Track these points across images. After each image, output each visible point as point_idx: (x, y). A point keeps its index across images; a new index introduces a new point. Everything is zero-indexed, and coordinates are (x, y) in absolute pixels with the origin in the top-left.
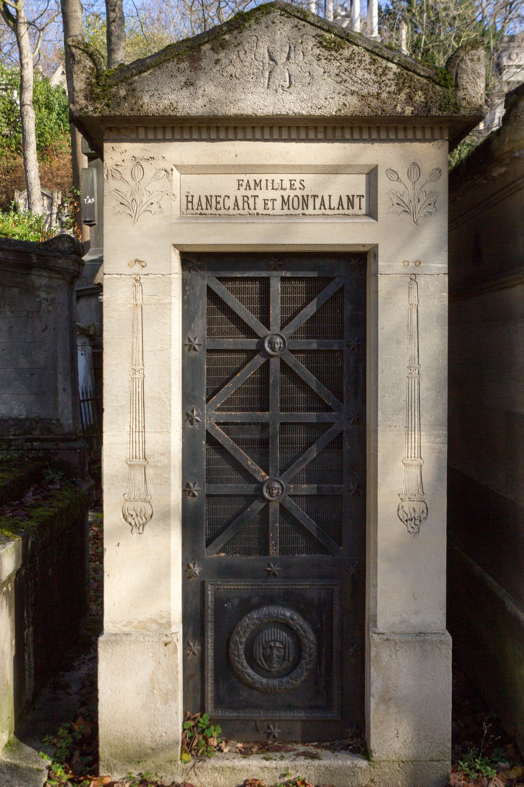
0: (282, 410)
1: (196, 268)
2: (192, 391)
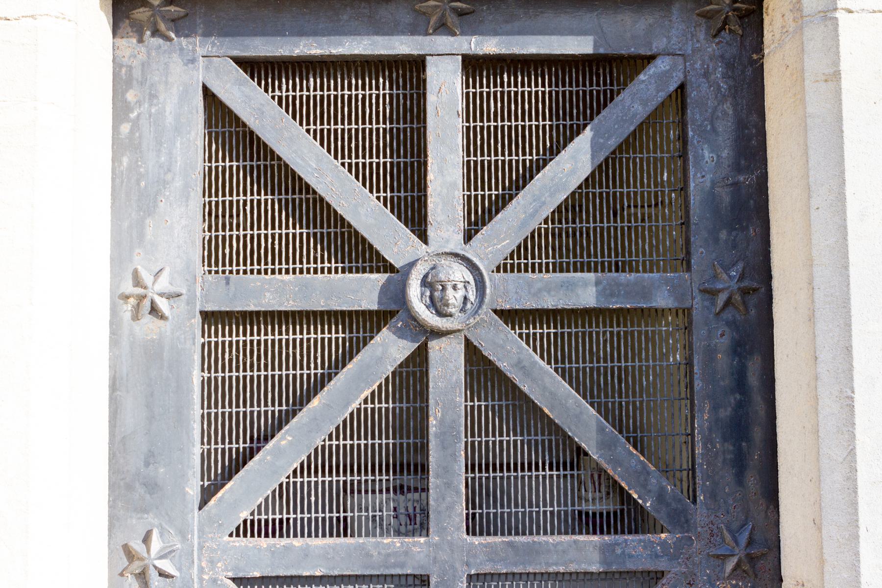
0: (475, 526)
1: (162, 26)
2: (147, 464)
